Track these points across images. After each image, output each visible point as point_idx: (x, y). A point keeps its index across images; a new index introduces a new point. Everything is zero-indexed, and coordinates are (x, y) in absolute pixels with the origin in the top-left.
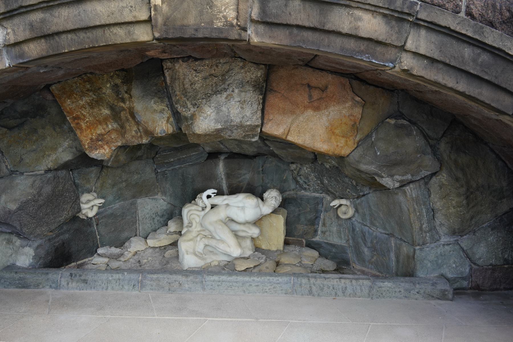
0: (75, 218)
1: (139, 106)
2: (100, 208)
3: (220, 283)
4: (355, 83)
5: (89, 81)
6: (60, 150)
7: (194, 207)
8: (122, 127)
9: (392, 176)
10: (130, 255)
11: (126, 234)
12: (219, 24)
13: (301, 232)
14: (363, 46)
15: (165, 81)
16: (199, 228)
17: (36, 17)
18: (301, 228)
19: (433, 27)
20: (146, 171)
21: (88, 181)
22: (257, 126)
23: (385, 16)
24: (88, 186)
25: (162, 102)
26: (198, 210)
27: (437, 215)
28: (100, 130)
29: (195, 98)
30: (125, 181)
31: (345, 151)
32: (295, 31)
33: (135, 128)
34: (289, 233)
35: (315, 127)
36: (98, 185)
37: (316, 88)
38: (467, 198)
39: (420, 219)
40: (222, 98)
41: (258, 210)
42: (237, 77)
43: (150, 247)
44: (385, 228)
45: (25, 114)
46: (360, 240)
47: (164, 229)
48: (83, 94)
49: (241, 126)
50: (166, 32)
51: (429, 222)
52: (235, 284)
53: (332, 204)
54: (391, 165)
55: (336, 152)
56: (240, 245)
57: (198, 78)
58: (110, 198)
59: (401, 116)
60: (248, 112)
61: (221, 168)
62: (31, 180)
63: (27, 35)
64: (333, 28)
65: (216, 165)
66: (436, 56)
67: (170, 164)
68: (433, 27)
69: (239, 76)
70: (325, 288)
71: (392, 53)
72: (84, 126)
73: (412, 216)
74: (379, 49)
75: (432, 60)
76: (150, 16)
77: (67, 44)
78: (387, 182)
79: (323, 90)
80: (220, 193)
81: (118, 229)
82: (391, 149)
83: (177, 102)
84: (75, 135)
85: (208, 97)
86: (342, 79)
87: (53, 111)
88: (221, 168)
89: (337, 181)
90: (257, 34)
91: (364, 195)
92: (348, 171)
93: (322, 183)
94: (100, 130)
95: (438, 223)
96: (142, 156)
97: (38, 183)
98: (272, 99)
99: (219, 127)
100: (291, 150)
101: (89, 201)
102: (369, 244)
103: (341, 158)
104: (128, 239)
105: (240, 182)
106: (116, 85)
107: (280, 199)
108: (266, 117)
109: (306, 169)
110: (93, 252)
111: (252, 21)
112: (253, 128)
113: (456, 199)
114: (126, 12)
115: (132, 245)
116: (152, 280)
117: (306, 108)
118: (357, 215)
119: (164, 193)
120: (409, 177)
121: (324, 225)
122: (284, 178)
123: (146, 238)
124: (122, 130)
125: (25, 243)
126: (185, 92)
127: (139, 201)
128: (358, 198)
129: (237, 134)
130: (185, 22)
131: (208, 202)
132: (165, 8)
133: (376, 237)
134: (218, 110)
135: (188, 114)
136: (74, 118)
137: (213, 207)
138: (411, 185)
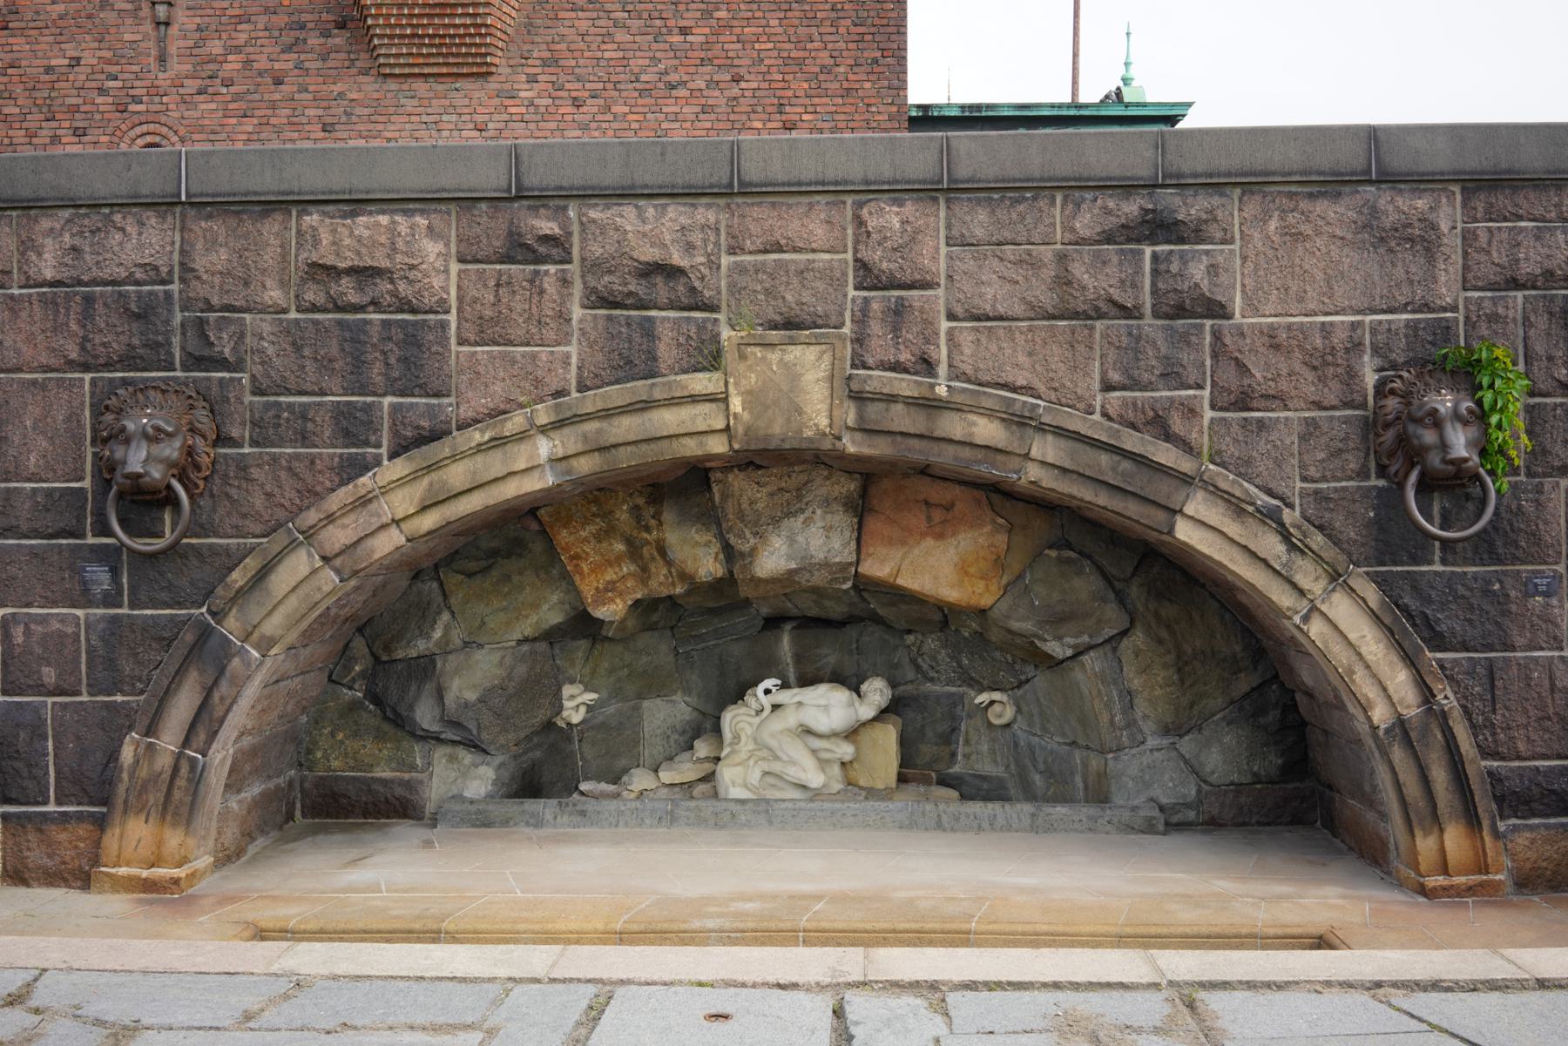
0: (549, 726)
1: (672, 537)
2: (590, 708)
4: (996, 498)
5: (596, 501)
7: (743, 710)
8: (645, 569)
9: (1060, 638)
10: (632, 796)
11: (623, 763)
12: (808, 433)
13: (927, 759)
14: (980, 454)
15: (712, 499)
16: (751, 746)
18: (927, 750)
19: (1060, 432)
20: (659, 650)
21: (573, 665)
22: (850, 564)
23: (1003, 420)
24: (571, 672)
25: (708, 530)
27: (1136, 701)
28: (610, 575)
29: (756, 524)
30: (628, 666)
31: (986, 601)
32: (899, 439)
33: (664, 571)
34: (904, 763)
36: (587, 670)
37: (937, 506)
38: (1179, 670)
41: (851, 710)
42: (819, 492)
44: (1064, 735)
45: (494, 553)
46: (1027, 762)
47: (687, 755)
48: (586, 521)
49: (825, 565)
50: (748, 443)
51: (1124, 712)
54: (1059, 620)
57: (761, 494)
58: (605, 695)
59: (1069, 546)
60: (836, 544)
61: (785, 644)
63: (580, 447)
64: (943, 435)
65: (778, 640)
66: (1067, 465)
67: (700, 638)
68: (1060, 432)
69: (823, 491)
70: (963, 817)
71: (1015, 462)
72: (586, 569)
73: (1096, 701)
74: (999, 457)
75: (1064, 470)
76: (728, 425)
77: (626, 459)
78: (1055, 648)
79: (949, 507)
80: (785, 685)
82: (1056, 596)
83: (730, 530)
84: (572, 583)
85: (776, 522)
86: (976, 493)
87: (538, 547)
88: (785, 644)
90: (853, 442)
91: (1028, 681)
92: (994, 635)
93: (960, 666)
94: (610, 575)
96: (656, 623)
97: (508, 660)
98: (872, 523)
99: (793, 566)
100: (903, 607)
101: (572, 697)
102: (1041, 767)
103: (983, 612)
104: (626, 771)
105: (818, 669)
106: (637, 508)
107: (888, 693)
108: (864, 550)
109: (931, 643)
111: (848, 428)
112: (844, 567)
113: (1163, 674)
114: (699, 420)
115: (635, 780)
116: (688, 809)
117: (923, 535)
118: (1019, 718)
119: (687, 691)
120: (1085, 639)
121: (967, 742)
123: (656, 771)
124: (644, 573)
125: (479, 758)
126: (741, 515)
127: (646, 704)
128: (1019, 687)
129: (819, 579)
130: (770, 432)
131: (767, 701)
132: (746, 416)
133: (1052, 752)
134: (791, 540)
135: (746, 548)
136: (572, 558)
137: (775, 707)
138: (1092, 653)
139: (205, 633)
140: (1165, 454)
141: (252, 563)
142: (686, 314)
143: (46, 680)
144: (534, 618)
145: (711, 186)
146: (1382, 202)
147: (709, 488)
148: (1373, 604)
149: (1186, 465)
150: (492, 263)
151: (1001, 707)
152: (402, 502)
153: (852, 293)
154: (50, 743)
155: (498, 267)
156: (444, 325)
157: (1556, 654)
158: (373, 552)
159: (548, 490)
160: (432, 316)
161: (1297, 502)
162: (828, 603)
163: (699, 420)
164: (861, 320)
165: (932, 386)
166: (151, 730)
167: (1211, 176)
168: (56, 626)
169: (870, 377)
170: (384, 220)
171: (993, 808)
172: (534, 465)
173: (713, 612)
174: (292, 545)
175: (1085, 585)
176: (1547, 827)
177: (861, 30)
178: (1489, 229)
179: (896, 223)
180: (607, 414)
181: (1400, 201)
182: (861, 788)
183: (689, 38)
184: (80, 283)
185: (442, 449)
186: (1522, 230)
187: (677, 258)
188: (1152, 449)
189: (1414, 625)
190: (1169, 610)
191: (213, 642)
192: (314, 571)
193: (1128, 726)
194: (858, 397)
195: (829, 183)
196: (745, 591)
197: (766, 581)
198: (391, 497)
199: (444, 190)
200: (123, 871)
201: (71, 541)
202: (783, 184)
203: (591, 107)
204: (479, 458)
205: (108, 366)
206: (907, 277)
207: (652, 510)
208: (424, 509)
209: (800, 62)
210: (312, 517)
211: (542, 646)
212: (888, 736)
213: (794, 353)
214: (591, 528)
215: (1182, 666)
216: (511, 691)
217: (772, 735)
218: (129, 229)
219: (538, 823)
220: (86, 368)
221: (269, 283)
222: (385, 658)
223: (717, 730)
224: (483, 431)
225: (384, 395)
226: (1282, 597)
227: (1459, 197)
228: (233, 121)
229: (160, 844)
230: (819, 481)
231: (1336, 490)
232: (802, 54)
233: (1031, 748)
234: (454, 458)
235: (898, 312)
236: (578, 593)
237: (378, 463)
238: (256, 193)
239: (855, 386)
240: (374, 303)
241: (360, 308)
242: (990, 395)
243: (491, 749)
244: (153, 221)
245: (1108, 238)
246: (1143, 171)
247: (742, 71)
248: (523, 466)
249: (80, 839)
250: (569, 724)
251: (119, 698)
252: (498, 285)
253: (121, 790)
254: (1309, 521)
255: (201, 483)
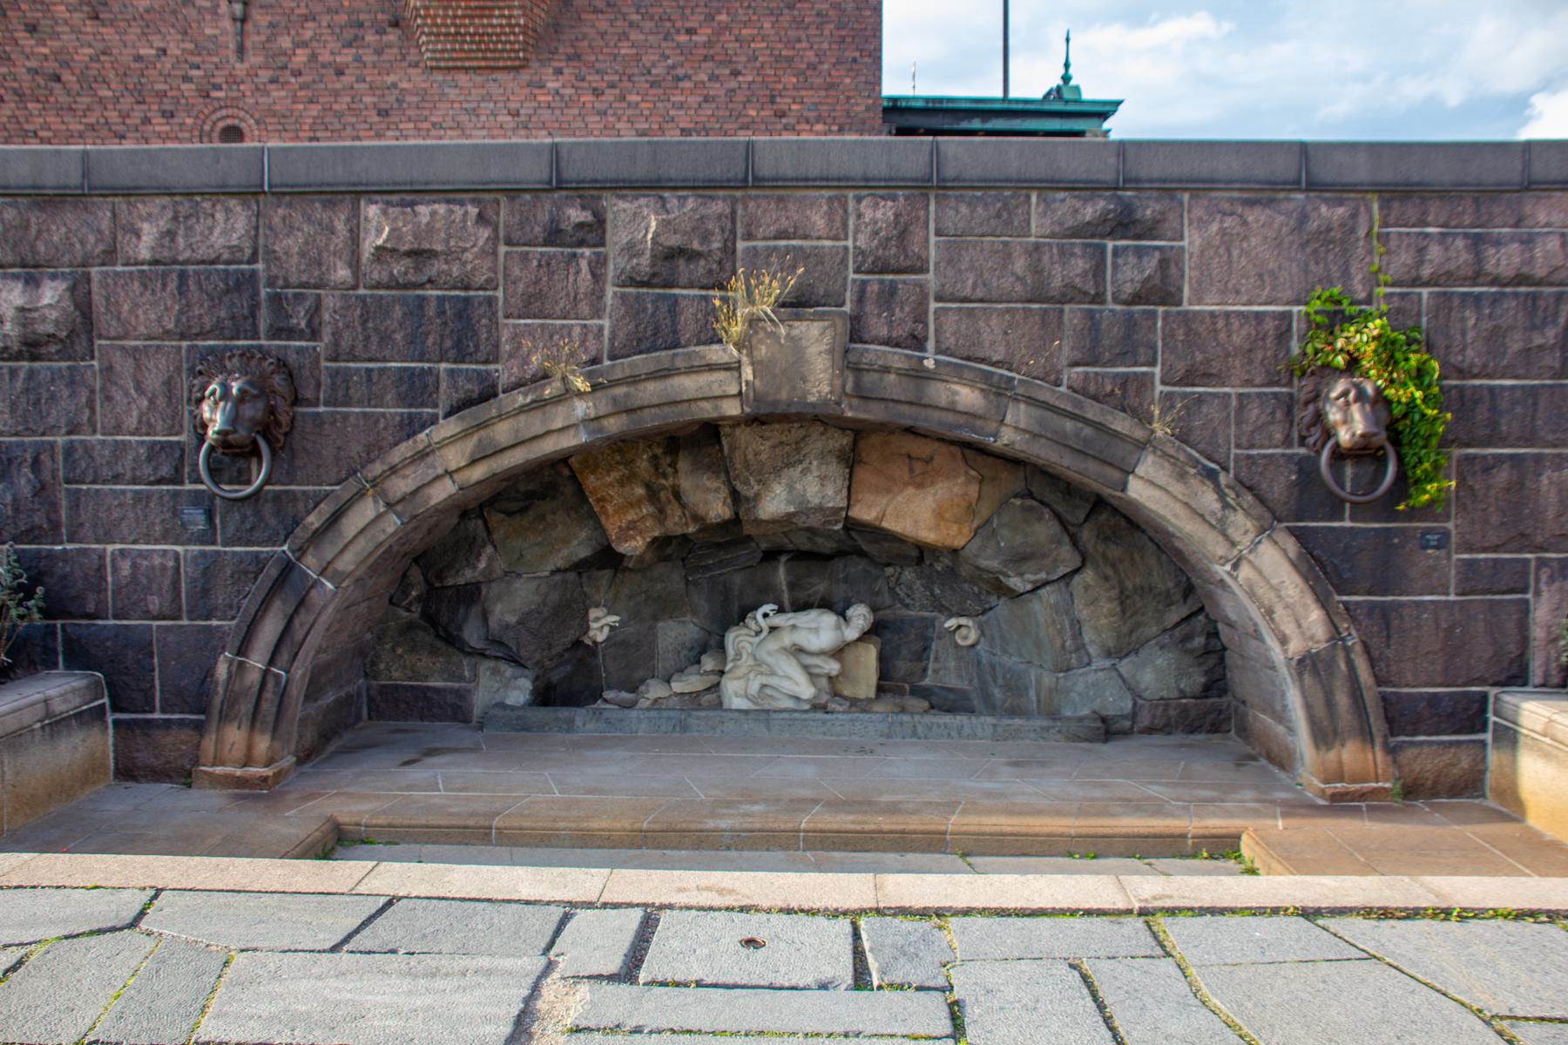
0: (578, 644)
1: (686, 483)
2: (612, 628)
4: (968, 452)
5: (619, 451)
6: (575, 542)
7: (745, 631)
8: (661, 511)
9: (1021, 575)
10: (648, 703)
11: (639, 674)
12: (812, 399)
16: (751, 662)
17: (620, 391)
18: (902, 666)
20: (672, 578)
24: (596, 597)
27: (1084, 629)
28: (632, 515)
29: (760, 472)
31: (959, 542)
32: (891, 405)
33: (679, 513)
34: (884, 674)
35: (917, 511)
37: (918, 459)
38: (1122, 603)
39: (1060, 632)
40: (795, 472)
43: (676, 694)
44: (1021, 655)
45: (530, 496)
46: (989, 679)
47: (694, 668)
48: (610, 469)
49: (820, 509)
53: (947, 625)
54: (1019, 559)
55: (948, 543)
56: (814, 684)
59: (1030, 495)
60: (830, 492)
61: (781, 574)
62: (535, 583)
63: (610, 409)
65: (776, 570)
67: (707, 568)
69: (819, 445)
72: (610, 510)
77: (651, 420)
78: (1016, 583)
80: (781, 610)
81: (633, 664)
82: (1019, 539)
84: (599, 522)
85: (777, 472)
86: (952, 448)
87: (569, 490)
88: (781, 574)
89: (953, 589)
90: (851, 408)
92: (964, 571)
93: (932, 594)
94: (632, 515)
95: (1087, 639)
98: (862, 474)
99: (792, 509)
100: (886, 545)
101: (597, 619)
102: (1000, 682)
103: (955, 551)
104: (643, 681)
106: (655, 457)
107: (870, 618)
109: (908, 574)
110: (596, 695)
113: (1108, 606)
114: (715, 386)
117: (906, 485)
119: (695, 613)
120: (1043, 576)
121: (937, 659)
123: (668, 682)
125: (519, 671)
127: (660, 624)
128: (983, 613)
129: (814, 521)
132: (757, 383)
133: (1010, 669)
134: (791, 488)
135: (751, 493)
136: (599, 500)
137: (773, 629)
138: (1048, 588)
139: (288, 569)
140: (1122, 424)
141: (326, 509)
142: (703, 293)
143: (151, 607)
144: (565, 552)
145: (729, 180)
146: (1309, 208)
147: (719, 442)
148: (1292, 555)
149: (1139, 434)
150: (535, 245)
151: (969, 633)
152: (454, 457)
153: (852, 276)
154: (156, 660)
155: (540, 249)
156: (491, 302)
157: (1443, 598)
158: (430, 498)
159: (581, 446)
160: (481, 293)
161: (1232, 465)
162: (820, 540)
163: (715, 386)
164: (860, 299)
165: (921, 359)
166: (243, 649)
167: (1164, 181)
168: (157, 561)
169: (867, 350)
170: (441, 209)
171: (960, 719)
172: (570, 424)
173: (719, 546)
174: (360, 495)
175: (1044, 530)
176: (1430, 743)
177: (843, 33)
178: (1400, 234)
179: (890, 214)
180: (634, 380)
181: (1323, 209)
182: (846, 698)
183: (694, 38)
184: (175, 262)
185: (490, 409)
186: (1427, 235)
187: (696, 245)
188: (1110, 418)
189: (1325, 573)
190: (1114, 552)
191: (295, 575)
192: (379, 517)
193: (1077, 650)
194: (857, 370)
195: (833, 179)
196: (748, 530)
197: (767, 522)
198: (445, 451)
199: (493, 182)
200: (219, 770)
201: (170, 487)
202: (792, 180)
203: (610, 95)
204: (522, 418)
205: (202, 335)
206: (903, 262)
207: (668, 460)
208: (473, 462)
209: (790, 60)
210: (378, 468)
211: (572, 576)
212: (869, 657)
213: (800, 328)
214: (615, 475)
215: (1123, 600)
216: (546, 614)
217: (769, 654)
218: (218, 216)
219: (570, 726)
220: (183, 337)
221: (339, 264)
222: (437, 585)
223: (721, 647)
224: (525, 395)
225: (440, 361)
226: (1217, 547)
227: (1376, 206)
228: (301, 107)
229: (250, 746)
230: (815, 435)
231: (1264, 456)
232: (790, 53)
233: (993, 666)
234: (501, 417)
235: (889, 293)
236: (603, 531)
237: (434, 420)
238: (329, 185)
239: (852, 358)
240: (430, 281)
241: (421, 286)
242: (971, 368)
243: (529, 664)
244: (239, 209)
245: (1076, 232)
246: (1108, 176)
247: (740, 67)
248: (560, 425)
249: (182, 742)
250: (595, 642)
251: (215, 623)
252: (540, 265)
253: (217, 700)
254: (1241, 482)
255: (282, 438)
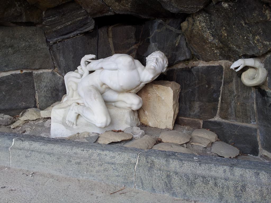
3: (28, 154)
26: (76, 77)
41: (134, 72)
52: (47, 157)
70: (199, 181)
122: (177, 45)
